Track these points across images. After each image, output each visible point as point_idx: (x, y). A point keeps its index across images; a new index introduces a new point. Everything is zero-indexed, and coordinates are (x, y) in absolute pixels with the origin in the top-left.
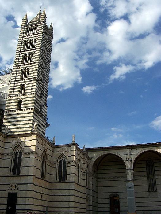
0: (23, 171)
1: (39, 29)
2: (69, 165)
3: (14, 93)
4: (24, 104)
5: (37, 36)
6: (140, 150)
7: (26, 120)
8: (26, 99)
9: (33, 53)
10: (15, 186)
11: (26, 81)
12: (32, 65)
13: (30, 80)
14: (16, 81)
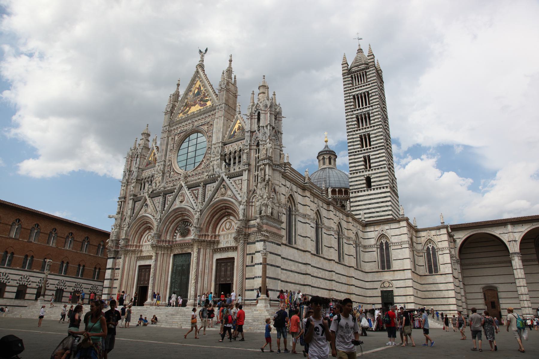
0: (396, 265)
1: (369, 76)
2: (440, 253)
3: (357, 168)
4: (375, 182)
5: (370, 87)
6: (529, 226)
7: (382, 202)
8: (376, 175)
9: (370, 112)
10: (389, 282)
11: (369, 150)
12: (372, 128)
13: (375, 149)
14: (356, 152)
